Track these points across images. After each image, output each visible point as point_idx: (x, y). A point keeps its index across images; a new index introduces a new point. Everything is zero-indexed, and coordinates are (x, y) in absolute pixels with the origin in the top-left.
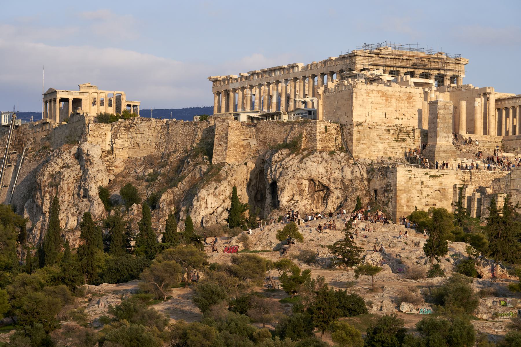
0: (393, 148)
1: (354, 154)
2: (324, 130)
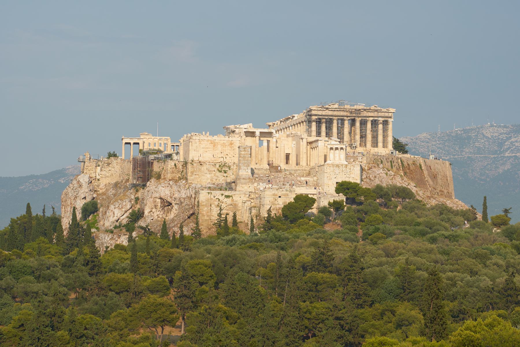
0: (218, 177)
1: (189, 182)
2: (174, 166)
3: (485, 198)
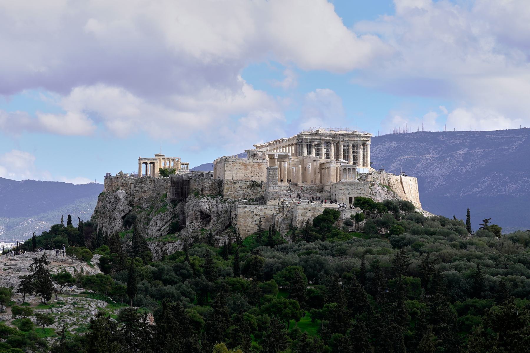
3: (468, 210)
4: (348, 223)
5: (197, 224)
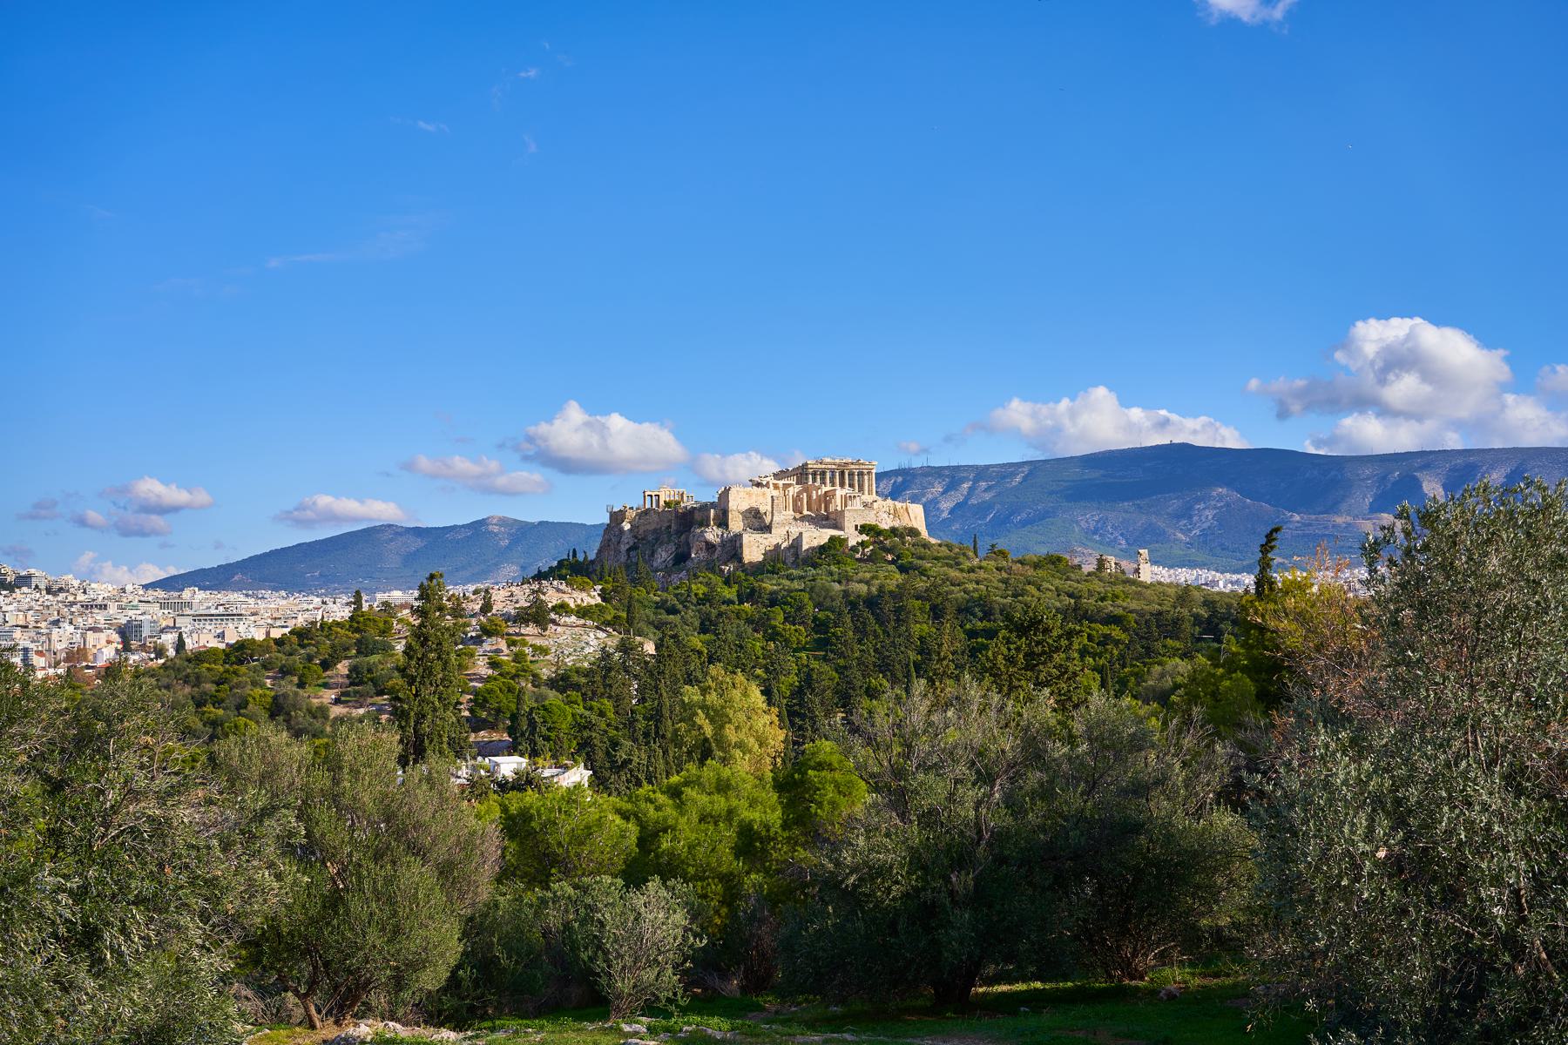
4: (854, 549)
5: (702, 555)
